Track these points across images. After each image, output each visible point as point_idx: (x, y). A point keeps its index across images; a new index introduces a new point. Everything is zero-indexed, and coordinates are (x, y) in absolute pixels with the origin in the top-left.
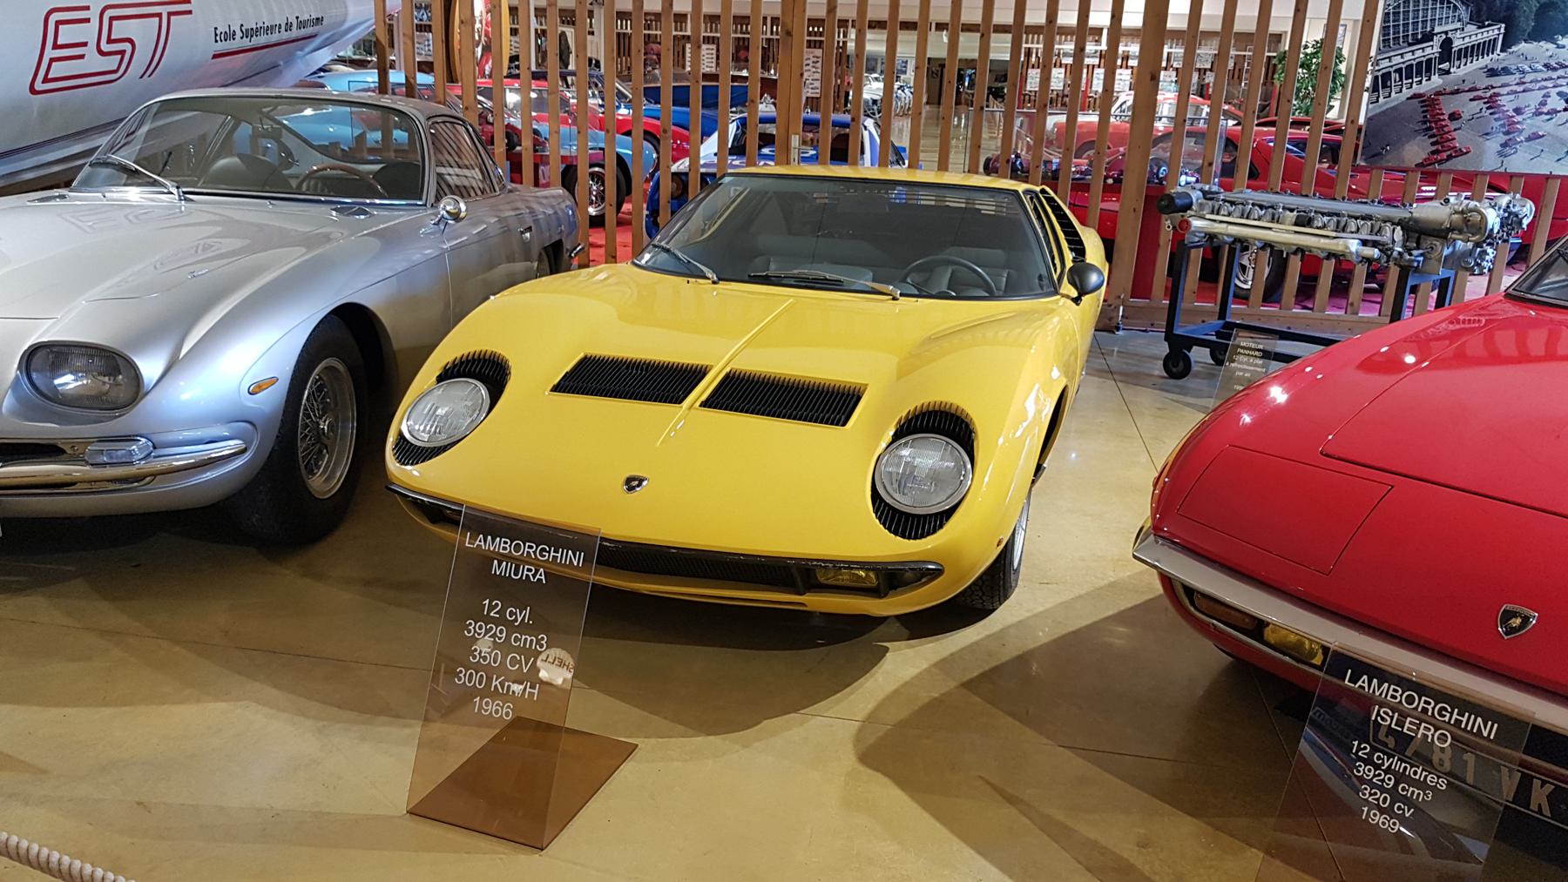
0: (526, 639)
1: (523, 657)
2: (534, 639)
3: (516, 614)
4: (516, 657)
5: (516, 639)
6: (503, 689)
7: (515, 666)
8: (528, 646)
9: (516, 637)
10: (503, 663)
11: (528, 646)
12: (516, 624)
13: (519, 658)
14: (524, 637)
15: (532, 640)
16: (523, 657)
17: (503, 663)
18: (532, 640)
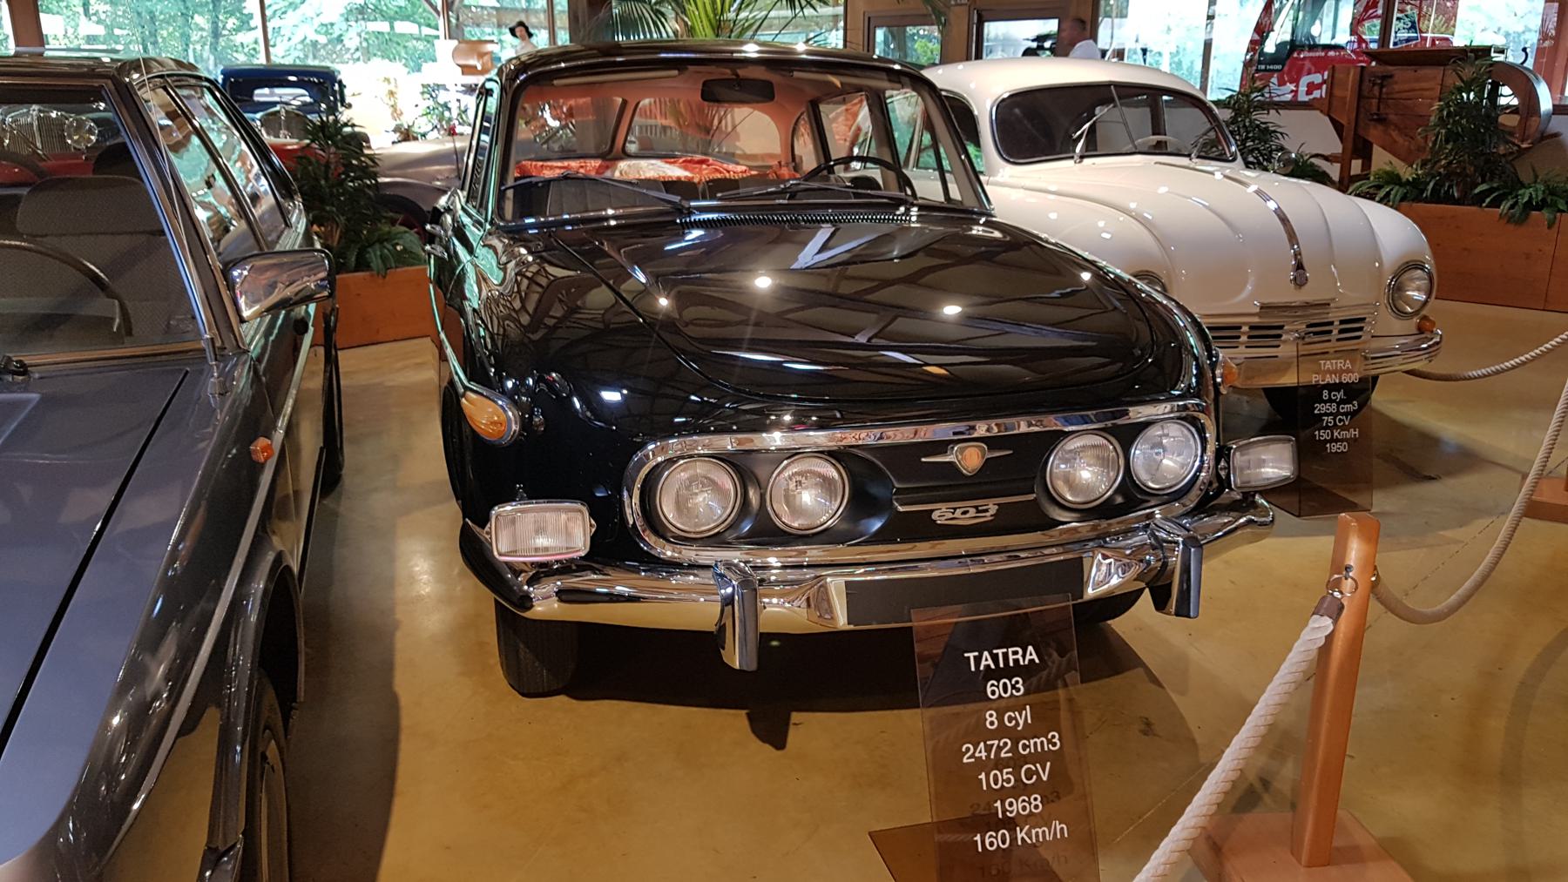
0: (1035, 743)
1: (1038, 765)
2: (1044, 739)
3: (1015, 718)
4: (1030, 768)
5: (1025, 747)
6: (1030, 838)
7: (1031, 779)
8: (1039, 750)
9: (1024, 744)
10: (1018, 780)
11: (1039, 750)
12: (1019, 728)
13: (1034, 768)
14: (1032, 742)
15: (1042, 743)
16: (1038, 765)
17: (1018, 780)
18: (1042, 743)
